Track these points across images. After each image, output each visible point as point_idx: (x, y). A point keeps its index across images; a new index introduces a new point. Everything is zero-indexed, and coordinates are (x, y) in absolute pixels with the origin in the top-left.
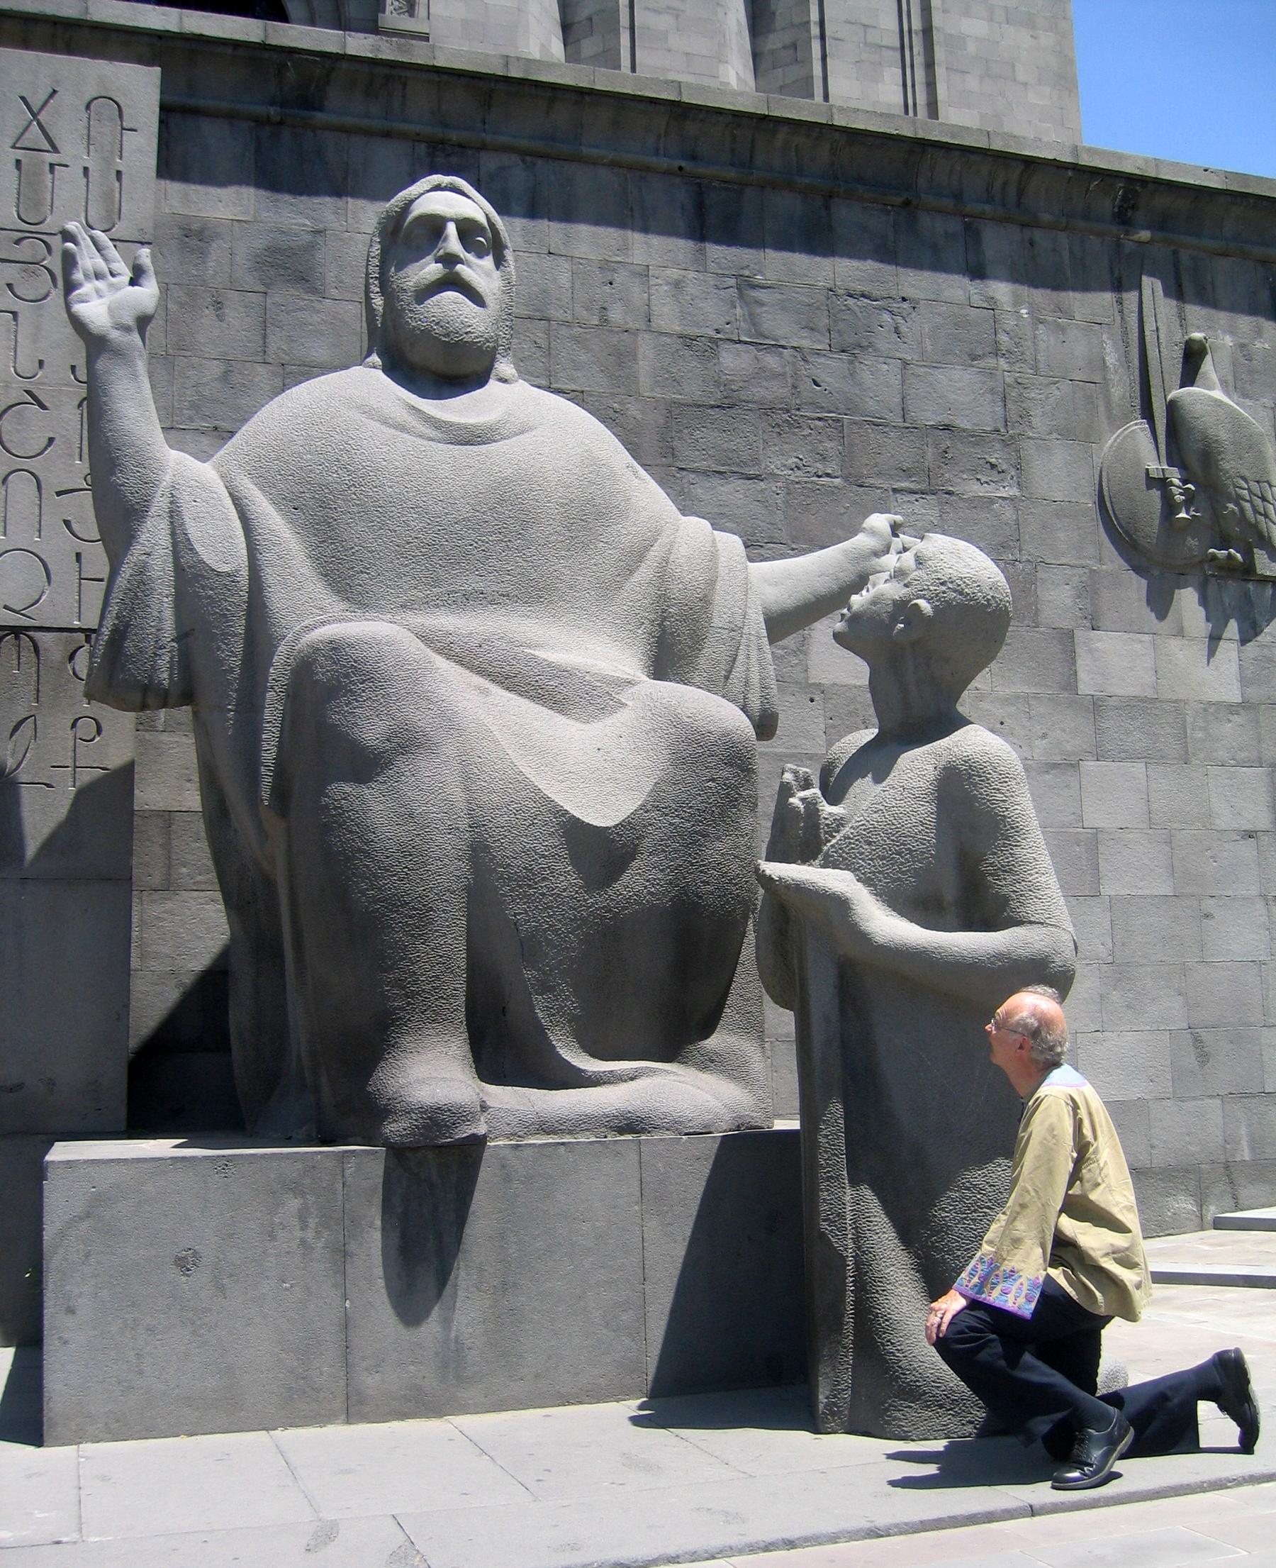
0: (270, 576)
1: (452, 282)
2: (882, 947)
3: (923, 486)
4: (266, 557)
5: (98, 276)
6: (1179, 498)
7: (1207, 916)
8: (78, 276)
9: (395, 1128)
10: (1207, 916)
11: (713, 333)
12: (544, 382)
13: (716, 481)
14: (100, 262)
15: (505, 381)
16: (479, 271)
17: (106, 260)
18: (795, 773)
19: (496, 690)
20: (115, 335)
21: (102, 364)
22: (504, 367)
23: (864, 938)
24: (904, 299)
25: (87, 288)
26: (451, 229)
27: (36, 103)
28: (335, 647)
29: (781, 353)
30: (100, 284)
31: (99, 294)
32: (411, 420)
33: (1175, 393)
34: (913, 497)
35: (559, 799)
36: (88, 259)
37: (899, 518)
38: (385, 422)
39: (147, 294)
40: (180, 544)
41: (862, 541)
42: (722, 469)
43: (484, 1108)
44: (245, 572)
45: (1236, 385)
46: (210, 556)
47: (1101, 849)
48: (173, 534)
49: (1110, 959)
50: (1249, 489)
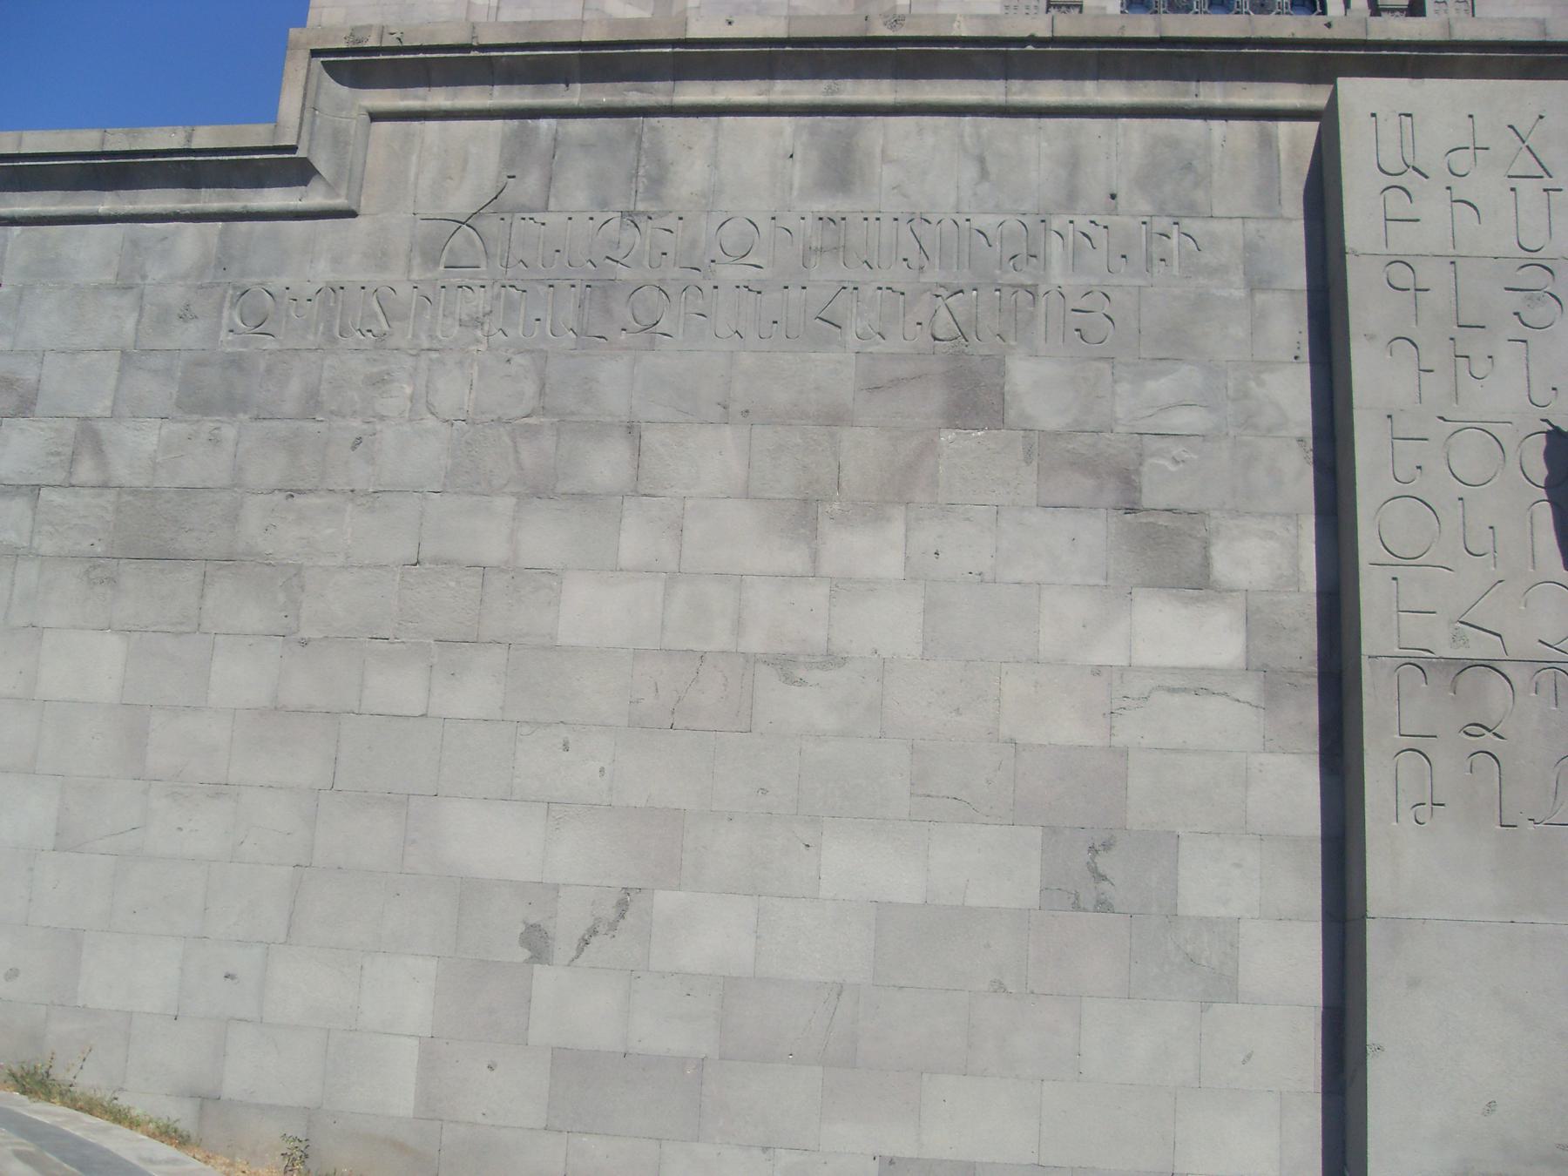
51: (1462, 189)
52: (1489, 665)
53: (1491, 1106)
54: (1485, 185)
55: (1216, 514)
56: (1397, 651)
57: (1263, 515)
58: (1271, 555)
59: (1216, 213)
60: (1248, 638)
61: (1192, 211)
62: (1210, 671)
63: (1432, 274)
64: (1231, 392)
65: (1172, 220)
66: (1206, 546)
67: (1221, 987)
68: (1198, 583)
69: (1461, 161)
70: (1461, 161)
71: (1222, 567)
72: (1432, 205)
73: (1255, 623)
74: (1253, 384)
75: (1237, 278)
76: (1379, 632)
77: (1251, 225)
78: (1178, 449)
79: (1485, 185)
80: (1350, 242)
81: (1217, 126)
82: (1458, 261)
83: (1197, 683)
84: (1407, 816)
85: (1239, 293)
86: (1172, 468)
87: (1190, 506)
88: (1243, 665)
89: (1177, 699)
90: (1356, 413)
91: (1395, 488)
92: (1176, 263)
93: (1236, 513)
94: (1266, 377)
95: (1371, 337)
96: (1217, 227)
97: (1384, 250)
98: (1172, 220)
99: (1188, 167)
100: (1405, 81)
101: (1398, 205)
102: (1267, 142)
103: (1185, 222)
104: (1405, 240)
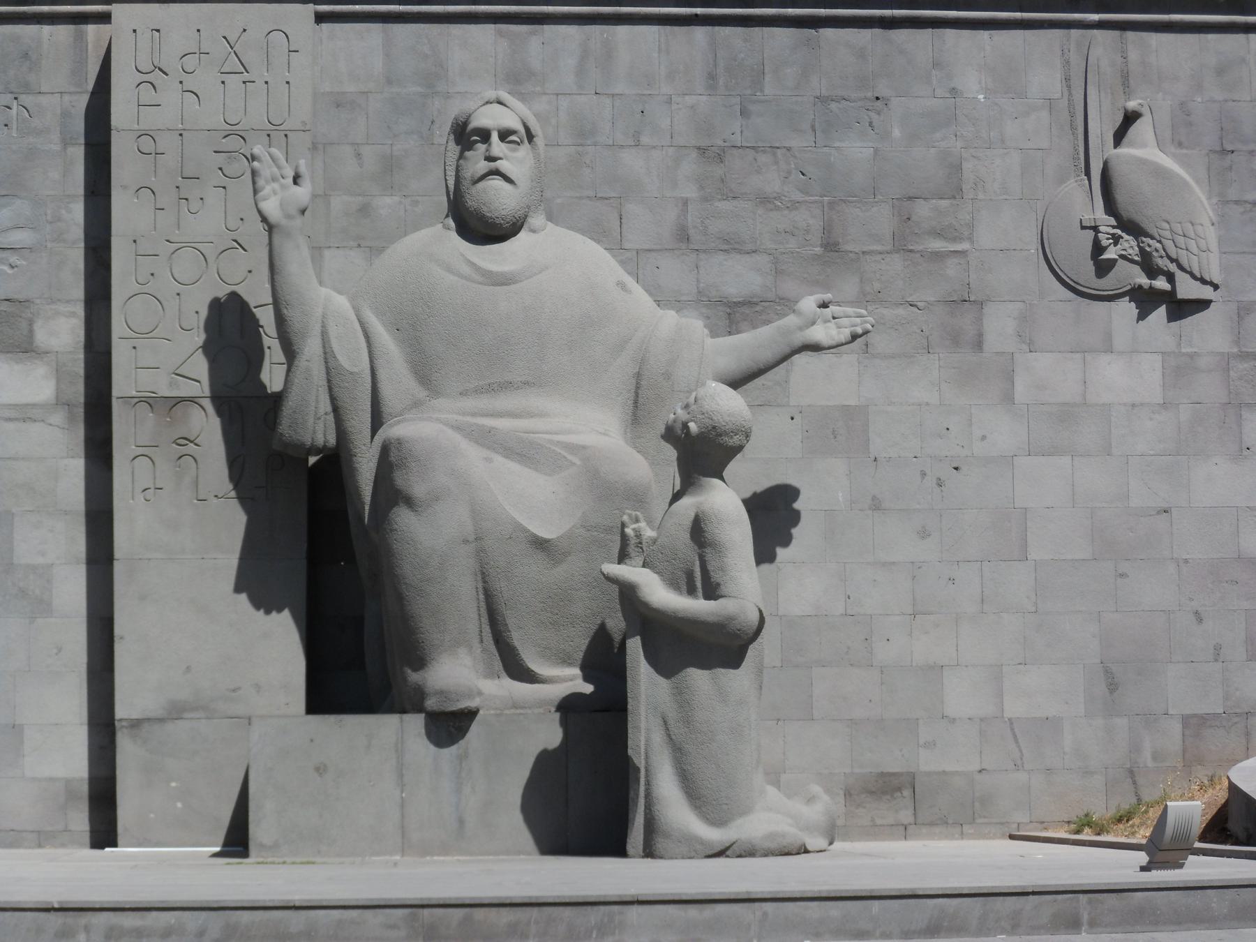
0: (382, 375)
1: (497, 172)
2: (657, 611)
3: (889, 247)
4: (379, 363)
5: (274, 179)
6: (1104, 243)
7: (1122, 575)
8: (260, 182)
9: (431, 704)
10: (1122, 575)
11: (720, 143)
12: (592, 194)
13: (721, 257)
14: (275, 169)
15: (534, 231)
16: (515, 161)
17: (279, 167)
18: (630, 515)
19: (499, 460)
20: (284, 222)
21: (277, 239)
22: (537, 220)
23: (646, 605)
24: (878, 98)
25: (267, 190)
26: (495, 137)
27: (232, 39)
28: (399, 442)
29: (774, 154)
30: (276, 186)
31: (275, 193)
32: (466, 270)
33: (1112, 152)
34: (879, 257)
35: (525, 523)
36: (265, 168)
37: (828, 296)
38: (449, 269)
39: (302, 193)
40: (328, 354)
41: (791, 320)
42: (726, 247)
43: (480, 693)
44: (368, 371)
45: (1179, 135)
46: (343, 360)
47: (1029, 524)
48: (324, 347)
49: (1033, 609)
50: (1171, 230)
51: (190, 83)
52: (192, 400)
53: (188, 669)
54: (205, 80)
55: (38, 301)
56: (134, 393)
57: (68, 302)
58: (63, 331)
59: (43, 90)
60: (58, 381)
61: (27, 88)
62: (33, 405)
63: (168, 143)
64: (49, 218)
65: (12, 96)
66: (31, 323)
67: (42, 607)
68: (25, 348)
69: (190, 62)
70: (190, 62)
71: (42, 337)
72: (170, 95)
73: (60, 373)
74: (63, 212)
75: (56, 137)
76: (122, 384)
77: (66, 98)
78: (14, 259)
79: (205, 80)
80: (113, 123)
81: (46, 29)
82: (184, 133)
83: (24, 414)
84: (140, 498)
85: (57, 147)
86: (10, 271)
87: (21, 297)
88: (54, 402)
89: (11, 426)
90: (113, 239)
91: (136, 288)
92: (15, 127)
93: (52, 301)
94: (72, 206)
95: (125, 187)
96: (43, 100)
97: (136, 127)
98: (12, 96)
99: (26, 56)
100: (157, 5)
101: (147, 94)
102: (80, 39)
103: (22, 97)
104: (152, 119)
